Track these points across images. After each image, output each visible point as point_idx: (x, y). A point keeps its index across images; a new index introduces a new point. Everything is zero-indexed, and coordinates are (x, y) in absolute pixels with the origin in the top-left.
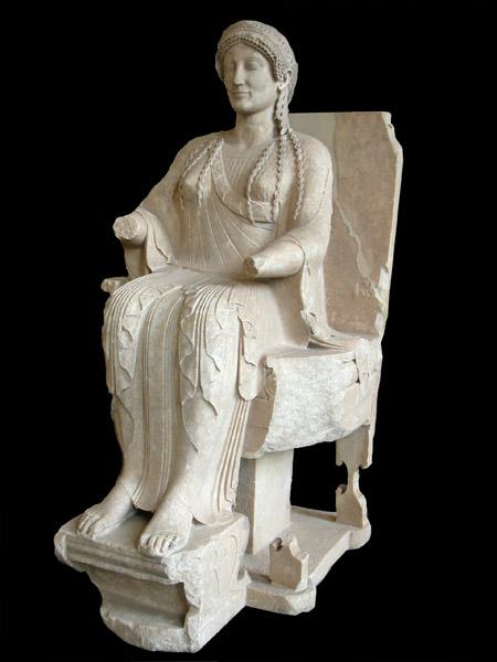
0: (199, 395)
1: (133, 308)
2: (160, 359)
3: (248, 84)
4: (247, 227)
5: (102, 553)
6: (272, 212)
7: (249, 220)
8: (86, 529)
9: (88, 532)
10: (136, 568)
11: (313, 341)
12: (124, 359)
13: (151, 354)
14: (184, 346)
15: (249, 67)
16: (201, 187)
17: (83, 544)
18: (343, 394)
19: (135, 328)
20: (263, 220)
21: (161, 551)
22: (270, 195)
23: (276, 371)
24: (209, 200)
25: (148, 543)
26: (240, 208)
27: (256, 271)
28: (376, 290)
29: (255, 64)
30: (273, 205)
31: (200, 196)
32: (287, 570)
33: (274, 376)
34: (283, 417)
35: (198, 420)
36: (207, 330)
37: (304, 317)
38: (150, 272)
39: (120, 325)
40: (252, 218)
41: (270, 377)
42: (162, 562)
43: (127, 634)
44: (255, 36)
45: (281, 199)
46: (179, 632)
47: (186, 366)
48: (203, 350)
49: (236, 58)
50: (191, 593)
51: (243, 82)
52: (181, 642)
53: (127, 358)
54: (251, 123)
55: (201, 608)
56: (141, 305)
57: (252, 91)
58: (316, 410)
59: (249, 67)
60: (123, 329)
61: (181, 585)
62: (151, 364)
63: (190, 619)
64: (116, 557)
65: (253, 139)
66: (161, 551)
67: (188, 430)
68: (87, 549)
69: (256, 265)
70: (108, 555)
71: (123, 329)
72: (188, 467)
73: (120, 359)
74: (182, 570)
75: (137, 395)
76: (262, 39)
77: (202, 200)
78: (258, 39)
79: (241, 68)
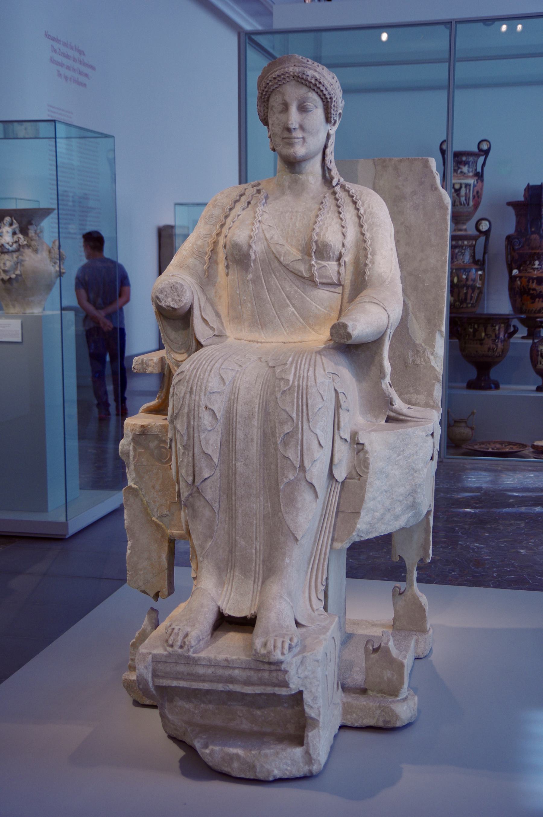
0: (301, 474)
2: (252, 440)
3: (302, 128)
5: (201, 671)
6: (339, 273)
7: (314, 281)
8: (179, 643)
10: (247, 682)
11: (392, 414)
12: (207, 443)
13: (240, 434)
15: (303, 109)
16: (254, 246)
18: (425, 471)
20: (329, 281)
21: (283, 654)
22: (337, 253)
23: (368, 447)
25: (265, 645)
26: (302, 268)
27: (349, 336)
28: (432, 357)
29: (309, 105)
30: (339, 265)
31: (253, 257)
32: (388, 674)
33: (367, 452)
34: (374, 499)
35: (299, 505)
36: (310, 402)
37: (384, 386)
38: (199, 345)
39: (203, 404)
40: (318, 280)
41: (361, 454)
42: (283, 666)
43: (236, 765)
44: (310, 73)
45: (348, 258)
46: (298, 751)
47: (286, 444)
48: (305, 427)
50: (311, 704)
51: (297, 126)
52: (301, 764)
53: (211, 442)
55: (321, 720)
56: (223, 379)
57: (305, 135)
58: (402, 490)
59: (303, 109)
60: (206, 407)
61: (301, 693)
62: (239, 445)
63: (310, 735)
64: (220, 672)
66: (283, 654)
68: (181, 668)
69: (350, 330)
70: (210, 671)
71: (206, 407)
72: (287, 560)
73: (203, 443)
74: (302, 676)
76: (318, 77)
77: (255, 260)
78: (313, 77)
79: (293, 109)
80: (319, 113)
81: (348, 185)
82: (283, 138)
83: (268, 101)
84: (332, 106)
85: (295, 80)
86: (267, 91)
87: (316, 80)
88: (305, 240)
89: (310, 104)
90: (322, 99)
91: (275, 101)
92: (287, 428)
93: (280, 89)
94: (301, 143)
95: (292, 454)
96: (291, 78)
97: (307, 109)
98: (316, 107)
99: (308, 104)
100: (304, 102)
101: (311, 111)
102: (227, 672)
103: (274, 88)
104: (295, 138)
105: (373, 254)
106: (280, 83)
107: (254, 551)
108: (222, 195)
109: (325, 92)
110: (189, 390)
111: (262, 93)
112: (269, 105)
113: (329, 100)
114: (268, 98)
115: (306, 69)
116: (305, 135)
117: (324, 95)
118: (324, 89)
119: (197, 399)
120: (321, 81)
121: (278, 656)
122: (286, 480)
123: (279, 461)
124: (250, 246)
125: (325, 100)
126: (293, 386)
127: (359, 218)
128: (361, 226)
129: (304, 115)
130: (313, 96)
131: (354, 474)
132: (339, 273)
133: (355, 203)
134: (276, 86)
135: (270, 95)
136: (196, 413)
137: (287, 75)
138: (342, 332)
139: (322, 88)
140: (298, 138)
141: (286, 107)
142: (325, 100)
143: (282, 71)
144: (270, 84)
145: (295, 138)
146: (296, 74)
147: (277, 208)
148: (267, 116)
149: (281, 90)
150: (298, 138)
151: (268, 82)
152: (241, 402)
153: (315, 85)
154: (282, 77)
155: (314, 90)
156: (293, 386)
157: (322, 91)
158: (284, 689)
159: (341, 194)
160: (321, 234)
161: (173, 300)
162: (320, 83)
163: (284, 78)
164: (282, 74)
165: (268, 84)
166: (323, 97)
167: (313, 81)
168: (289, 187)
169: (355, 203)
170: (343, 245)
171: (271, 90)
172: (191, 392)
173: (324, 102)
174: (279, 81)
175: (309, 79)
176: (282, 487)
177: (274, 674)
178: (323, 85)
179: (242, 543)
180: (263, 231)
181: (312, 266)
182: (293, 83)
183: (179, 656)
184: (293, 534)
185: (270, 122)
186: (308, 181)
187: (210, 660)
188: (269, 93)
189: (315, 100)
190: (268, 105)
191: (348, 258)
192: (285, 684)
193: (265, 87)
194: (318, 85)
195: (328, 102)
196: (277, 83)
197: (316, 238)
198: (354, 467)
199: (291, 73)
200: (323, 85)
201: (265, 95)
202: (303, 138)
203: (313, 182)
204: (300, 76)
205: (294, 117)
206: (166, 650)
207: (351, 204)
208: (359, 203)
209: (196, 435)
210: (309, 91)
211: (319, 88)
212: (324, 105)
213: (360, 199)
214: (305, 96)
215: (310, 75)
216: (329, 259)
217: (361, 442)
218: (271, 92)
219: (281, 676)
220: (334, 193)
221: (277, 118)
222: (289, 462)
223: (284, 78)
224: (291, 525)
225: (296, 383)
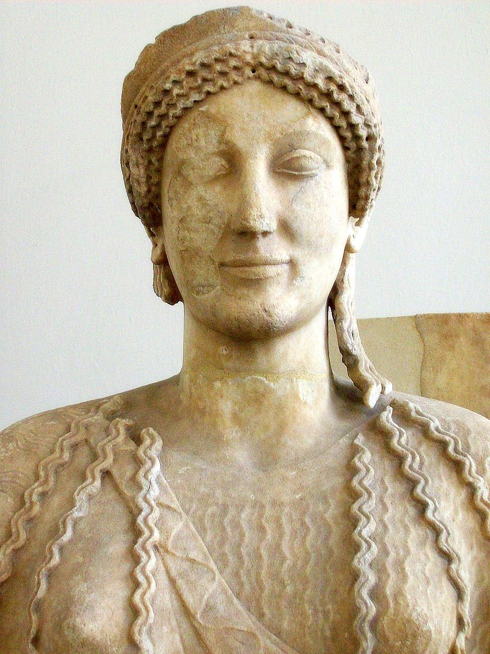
3: (287, 229)
15: (287, 168)
29: (309, 156)
54: (270, 372)
57: (298, 253)
59: (287, 168)
65: (282, 428)
76: (336, 71)
80: (331, 182)
81: (416, 404)
82: (222, 265)
83: (163, 145)
84: (374, 162)
85: (258, 78)
86: (162, 117)
87: (330, 79)
88: (326, 614)
89: (313, 154)
90: (342, 139)
91: (194, 146)
94: (284, 279)
96: (248, 72)
97: (301, 169)
98: (328, 166)
99: (307, 153)
100: (292, 148)
101: (311, 177)
103: (189, 103)
104: (266, 263)
106: (208, 88)
108: (11, 446)
109: (356, 119)
111: (144, 124)
112: (169, 157)
113: (365, 144)
114: (166, 137)
115: (295, 46)
116: (298, 253)
117: (352, 127)
118: (353, 110)
120: (346, 81)
125: (353, 145)
134: (195, 97)
135: (172, 127)
137: (233, 63)
139: (348, 105)
140: (275, 263)
142: (353, 145)
143: (216, 51)
144: (176, 91)
145: (266, 263)
146: (263, 60)
147: (202, 489)
148: (158, 196)
149: (213, 110)
150: (275, 263)
151: (168, 86)
153: (328, 95)
154: (218, 67)
155: (322, 110)
157: (346, 114)
159: (403, 439)
160: (388, 591)
162: (342, 88)
163: (223, 74)
164: (217, 60)
165: (167, 92)
166: (348, 135)
167: (320, 82)
168: (236, 419)
169: (457, 466)
170: (460, 622)
171: (178, 112)
173: (345, 149)
174: (205, 80)
175: (308, 74)
178: (351, 97)
180: (172, 581)
182: (255, 87)
185: (170, 213)
186: (296, 396)
188: (171, 121)
189: (325, 142)
190: (161, 160)
193: (157, 104)
194: (335, 96)
195: (360, 149)
196: (198, 89)
199: (248, 58)
200: (351, 97)
201: (154, 127)
202: (292, 264)
203: (310, 400)
204: (279, 66)
205: (266, 199)
207: (443, 470)
210: (307, 114)
211: (338, 104)
212: (347, 160)
213: (467, 448)
214: (297, 127)
215: (309, 63)
218: (178, 118)
221: (201, 199)
223: (223, 74)
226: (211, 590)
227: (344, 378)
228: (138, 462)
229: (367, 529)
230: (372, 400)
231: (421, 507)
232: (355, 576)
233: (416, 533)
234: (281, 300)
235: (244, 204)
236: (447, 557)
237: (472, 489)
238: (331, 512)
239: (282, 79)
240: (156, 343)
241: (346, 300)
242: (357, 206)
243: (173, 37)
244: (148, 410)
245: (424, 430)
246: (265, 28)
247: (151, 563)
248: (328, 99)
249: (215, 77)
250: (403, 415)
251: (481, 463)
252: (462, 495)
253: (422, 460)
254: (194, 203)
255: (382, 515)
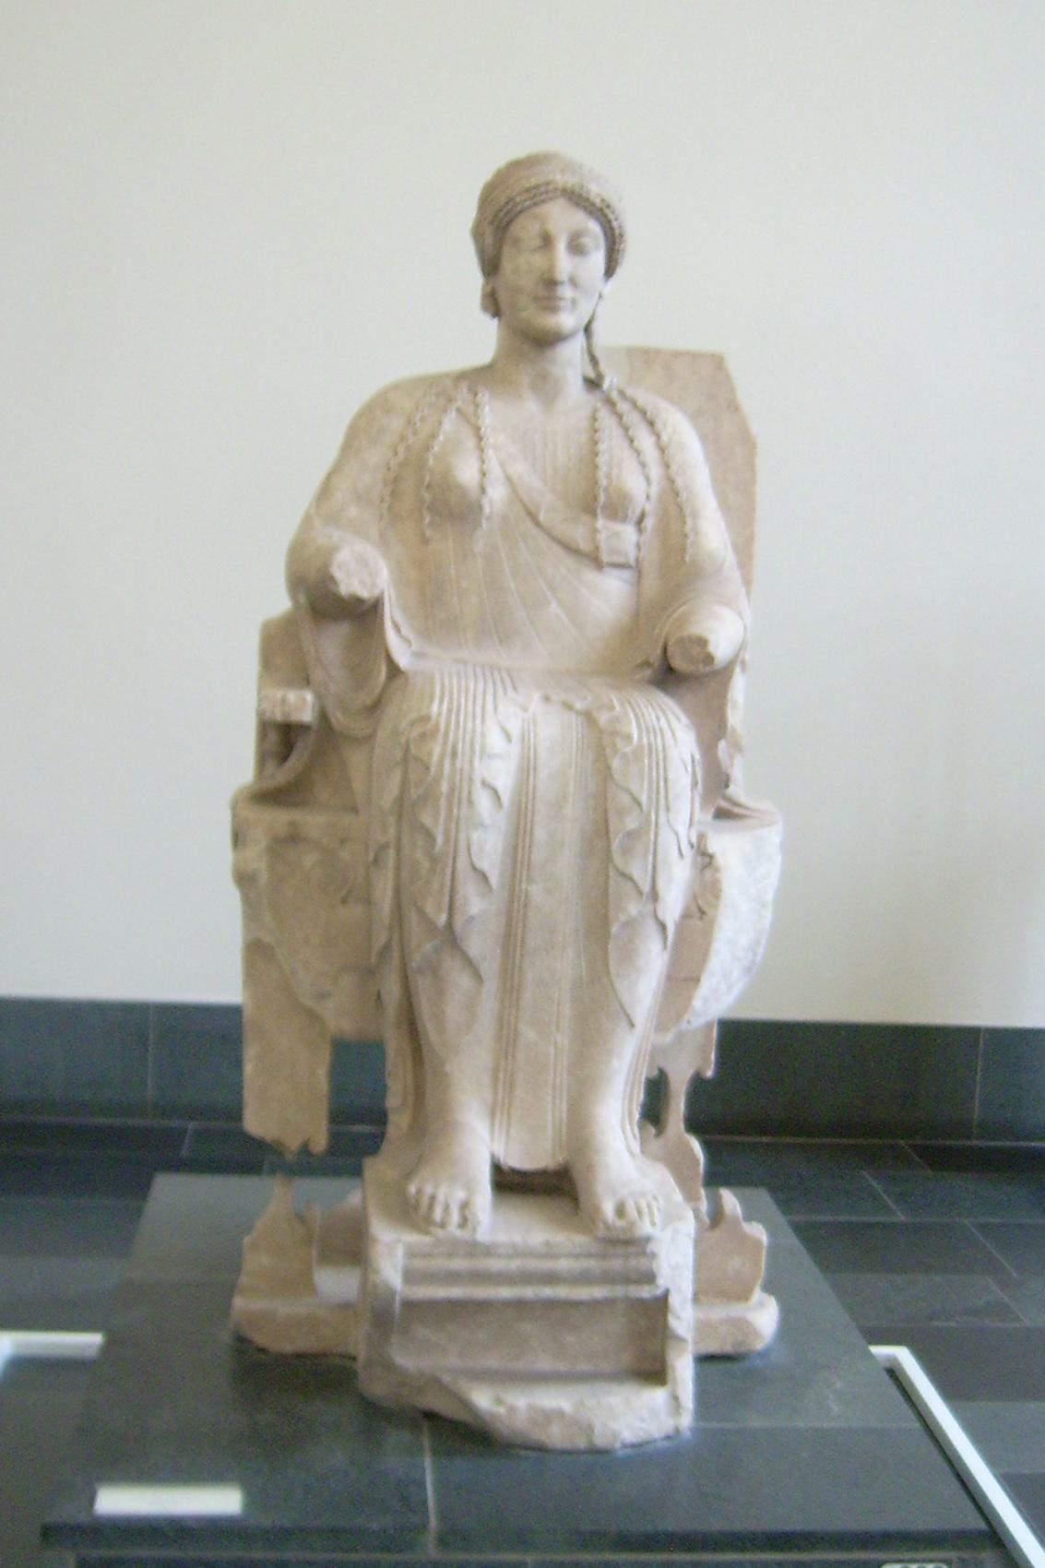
0: (649, 907)
1: (495, 741)
3: (574, 282)
4: (590, 575)
5: (495, 1265)
8: (455, 1217)
9: (464, 1222)
10: (583, 1279)
11: (724, 804)
13: (540, 834)
14: (621, 813)
15: (576, 248)
17: (450, 1255)
19: (502, 774)
20: (622, 560)
21: (653, 1224)
22: (638, 511)
23: (720, 860)
24: (505, 519)
25: (621, 1211)
26: (579, 535)
29: (586, 241)
31: (487, 510)
41: (708, 873)
47: (626, 851)
48: (662, 820)
49: (552, 227)
59: (576, 248)
60: (485, 784)
62: (538, 854)
64: (534, 1265)
66: (653, 1224)
67: (621, 986)
68: (458, 1264)
69: (711, 648)
70: (513, 1265)
75: (495, 926)
77: (489, 518)
79: (561, 247)
80: (598, 258)
81: (629, 392)
91: (526, 229)
92: (632, 823)
93: (537, 210)
95: (639, 871)
102: (546, 1265)
105: (695, 515)
107: (552, 1050)
110: (449, 750)
119: (467, 766)
121: (645, 1228)
122: (623, 918)
123: (611, 882)
124: (483, 490)
126: (640, 746)
127: (662, 450)
128: (667, 466)
129: (577, 260)
130: (594, 227)
131: (694, 908)
132: (638, 547)
133: (651, 424)
136: (465, 794)
138: (695, 651)
141: (547, 241)
152: (543, 773)
156: (640, 746)
158: (646, 1288)
159: (623, 407)
161: (363, 583)
167: (598, 201)
169: (651, 424)
170: (648, 497)
172: (454, 755)
176: (614, 929)
177: (633, 1262)
179: (528, 1034)
181: (595, 531)
183: (456, 1242)
184: (628, 1016)
185: (507, 266)
187: (514, 1246)
191: (649, 523)
192: (650, 1278)
197: (604, 482)
198: (695, 898)
205: (564, 263)
206: (427, 1233)
208: (659, 425)
209: (462, 837)
216: (624, 519)
217: (711, 850)
219: (642, 1263)
220: (610, 403)
222: (630, 884)
224: (625, 999)
225: (645, 741)
226: (520, 469)
227: (591, 374)
228: (477, 406)
229: (602, 447)
230: (606, 385)
231: (632, 441)
232: (596, 467)
233: (627, 452)
234: (567, 320)
235: (551, 268)
236: (643, 465)
237: (658, 437)
238: (584, 438)
239: (578, 199)
240: (480, 339)
241: (596, 327)
242: (610, 271)
243: (516, 166)
244: (476, 378)
245: (634, 404)
246: (569, 167)
247: (490, 453)
248: (602, 214)
249: (540, 194)
250: (622, 394)
251: (664, 425)
252: (653, 439)
253: (632, 418)
254: (521, 265)
255: (611, 440)
